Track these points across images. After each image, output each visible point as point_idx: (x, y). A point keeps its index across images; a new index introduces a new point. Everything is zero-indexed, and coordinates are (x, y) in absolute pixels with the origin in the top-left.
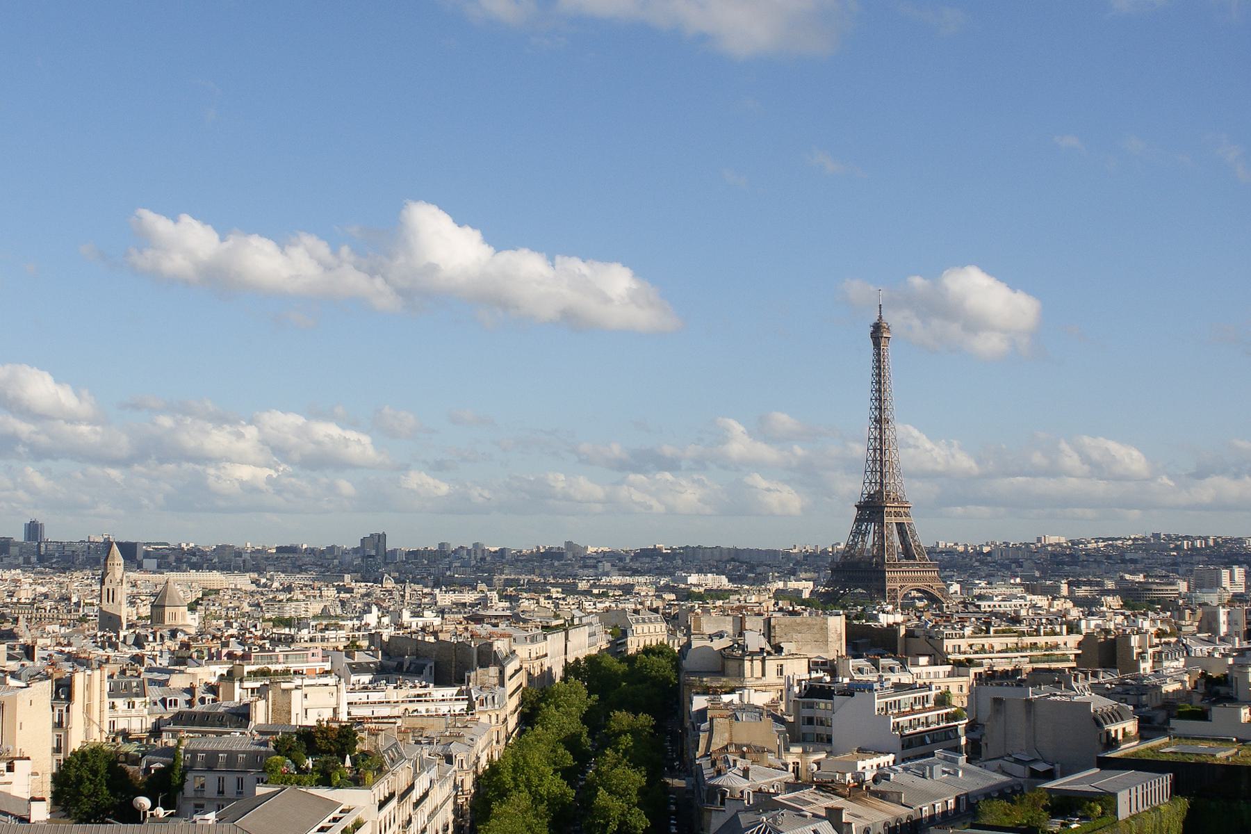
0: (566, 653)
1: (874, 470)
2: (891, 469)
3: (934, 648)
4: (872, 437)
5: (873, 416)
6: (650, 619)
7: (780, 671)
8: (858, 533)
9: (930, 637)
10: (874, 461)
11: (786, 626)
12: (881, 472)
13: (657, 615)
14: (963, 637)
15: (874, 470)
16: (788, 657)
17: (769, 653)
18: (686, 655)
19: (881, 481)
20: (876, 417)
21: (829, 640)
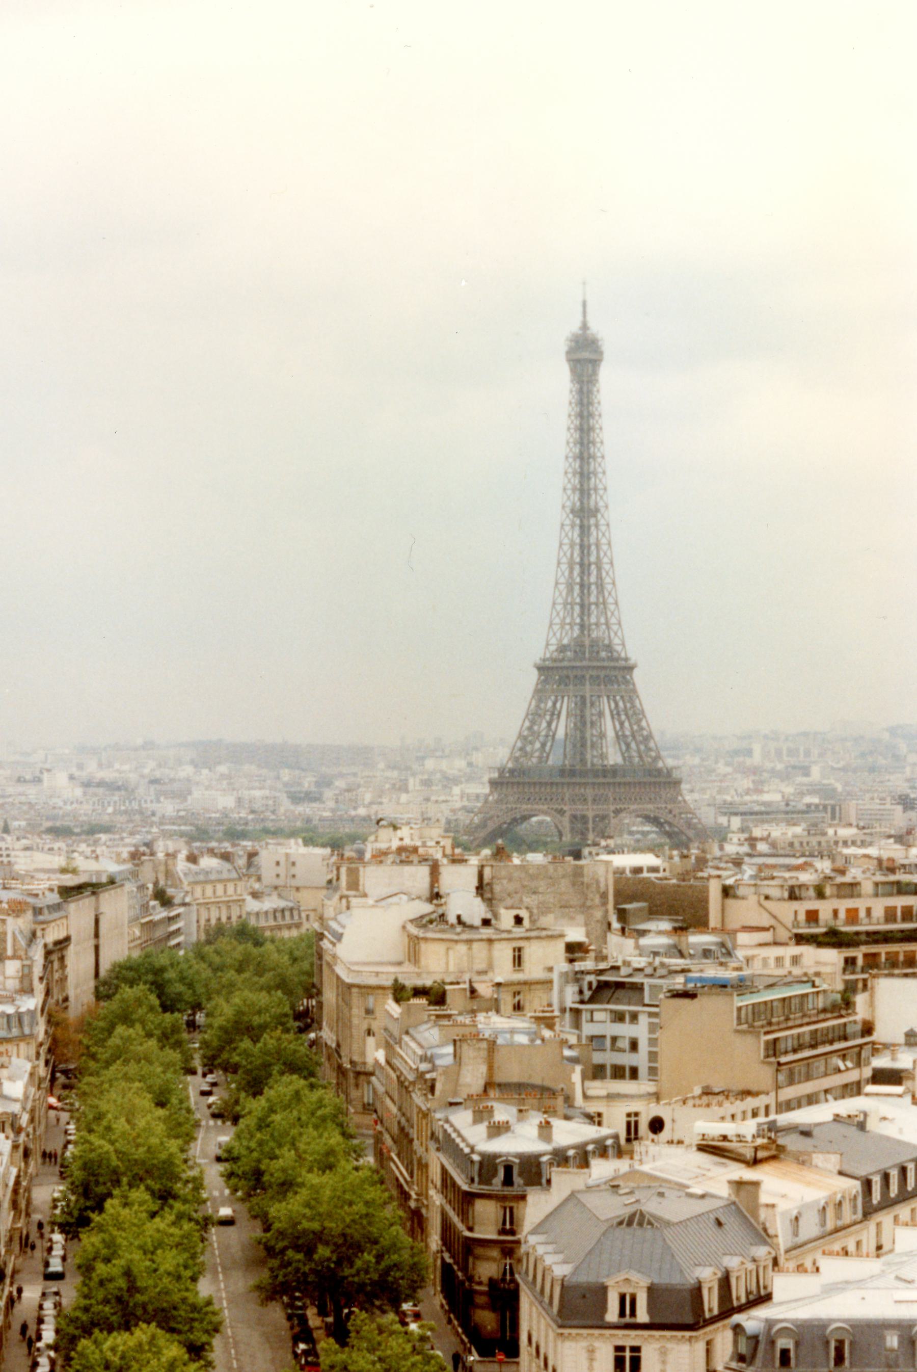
2: (601, 600)
3: (775, 917)
4: (566, 541)
5: (568, 504)
7: (518, 960)
8: (534, 716)
9: (767, 898)
12: (582, 606)
20: (574, 504)
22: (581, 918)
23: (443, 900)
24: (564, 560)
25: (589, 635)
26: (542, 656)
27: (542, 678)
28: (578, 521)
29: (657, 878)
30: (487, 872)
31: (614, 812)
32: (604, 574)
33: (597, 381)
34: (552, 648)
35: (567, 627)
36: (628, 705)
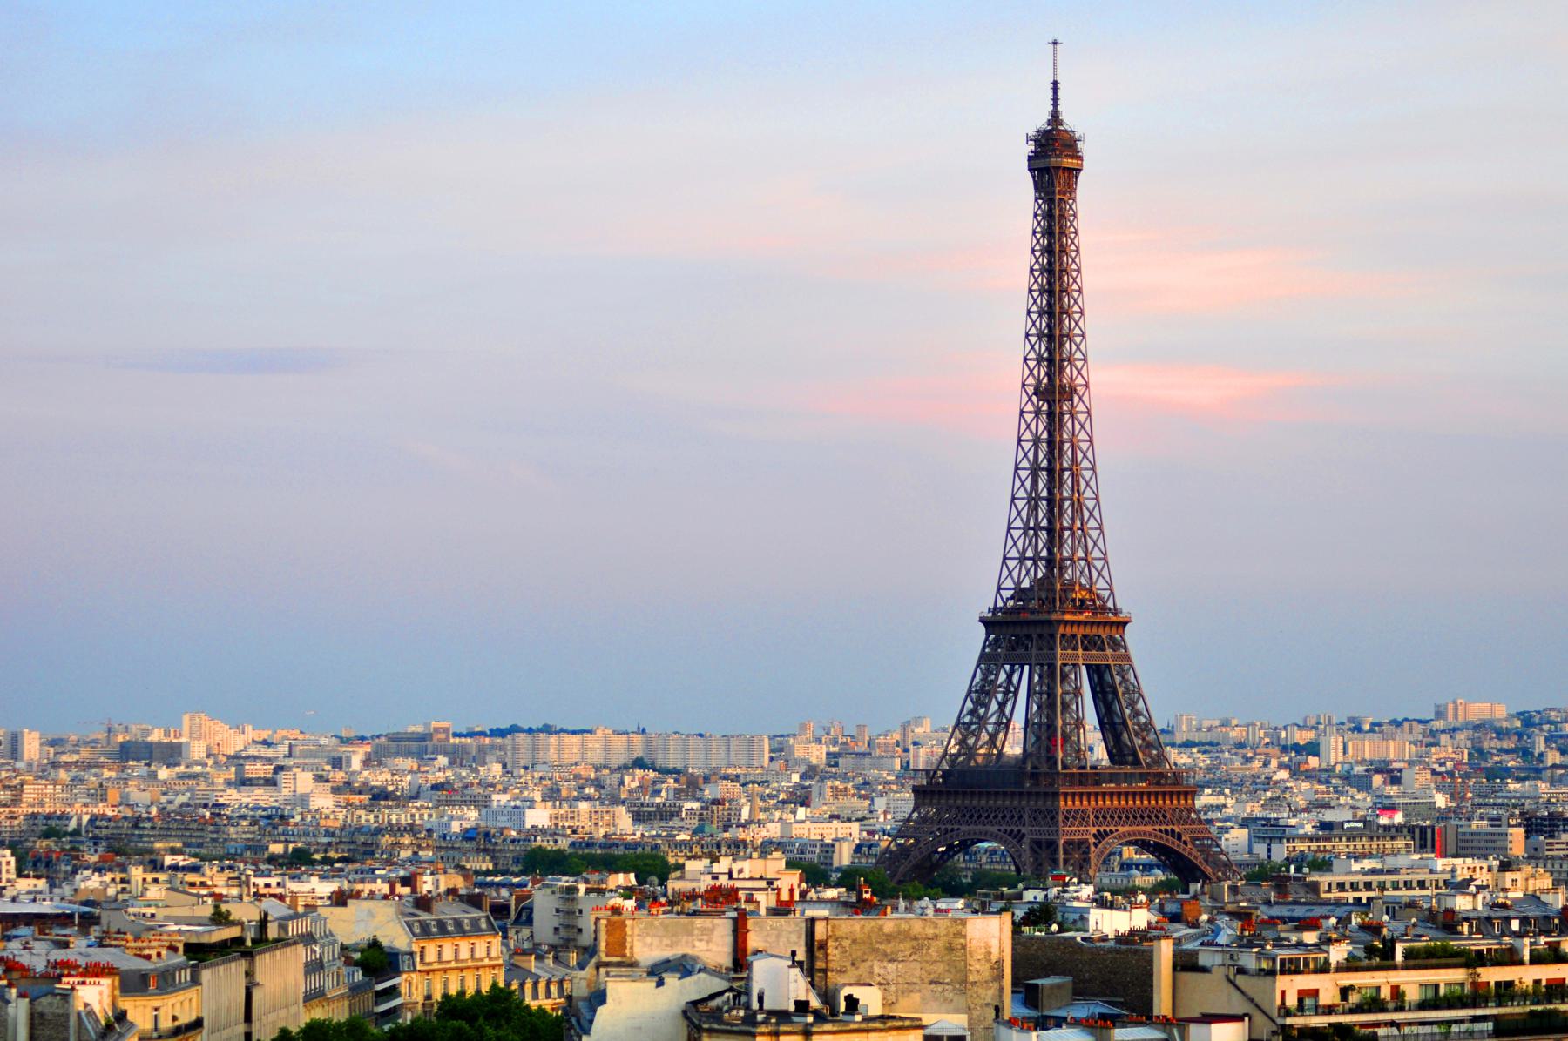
0: (248, 1018)
1: (1032, 524)
2: (1078, 523)
3: (1252, 1000)
4: (1027, 436)
5: (1031, 381)
6: (458, 923)
8: (981, 693)
9: (1241, 971)
10: (1033, 502)
11: (854, 941)
13: (476, 913)
14: (1324, 969)
15: (1032, 524)
16: (872, 1025)
17: (819, 1017)
18: (591, 1022)
19: (1050, 552)
20: (1039, 382)
21: (971, 978)
22: (960, 1001)
23: (744, 975)
24: (1025, 464)
25: (1061, 574)
26: (992, 607)
27: (992, 636)
28: (1045, 408)
29: (1083, 939)
30: (820, 930)
31: (1094, 835)
33: (1074, 201)
34: (1007, 594)
35: (1029, 563)
36: (1118, 679)
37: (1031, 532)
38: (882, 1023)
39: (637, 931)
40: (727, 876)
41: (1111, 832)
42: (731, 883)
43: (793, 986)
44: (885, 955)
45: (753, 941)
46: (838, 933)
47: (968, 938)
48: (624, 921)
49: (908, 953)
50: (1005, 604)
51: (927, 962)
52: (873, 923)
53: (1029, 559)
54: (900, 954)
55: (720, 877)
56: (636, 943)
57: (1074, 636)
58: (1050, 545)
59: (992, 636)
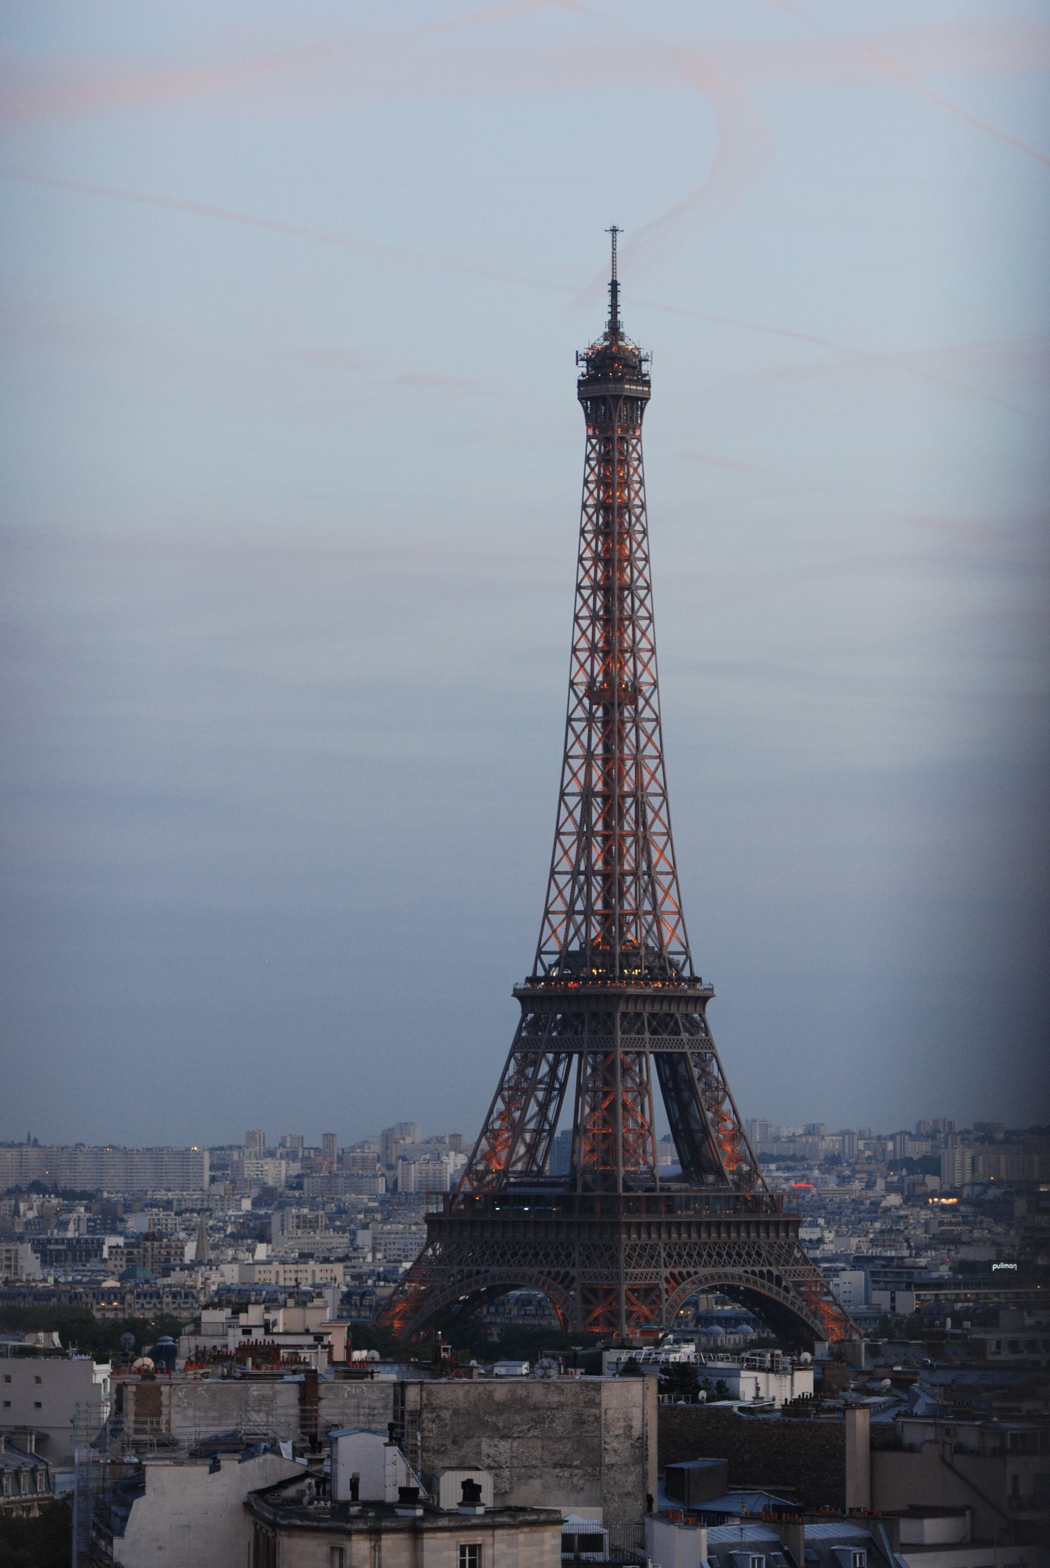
1: (582, 868)
4: (577, 750)
5: (582, 678)
9: (960, 1449)
10: (584, 836)
11: (456, 1412)
12: (607, 876)
15: (582, 868)
16: (500, 1519)
18: (125, 1519)
19: (607, 904)
20: (592, 679)
21: (608, 1459)
24: (574, 788)
25: (622, 934)
26: (530, 975)
27: (531, 1016)
28: (600, 713)
30: (412, 1395)
31: (666, 1279)
32: (650, 815)
33: (639, 440)
35: (579, 918)
36: (696, 1072)
37: (582, 878)
38: (511, 1516)
39: (174, 1400)
40: (262, 1330)
41: (689, 1274)
42: (269, 1339)
43: (389, 1469)
44: (497, 1430)
45: (327, 1411)
46: (436, 1402)
47: (603, 1406)
48: (158, 1388)
49: (526, 1427)
50: (547, 971)
51: (550, 1439)
52: (481, 1388)
53: (579, 913)
54: (516, 1429)
55: (254, 1330)
56: (173, 1416)
57: (639, 1015)
58: (607, 895)
59: (531, 1016)
